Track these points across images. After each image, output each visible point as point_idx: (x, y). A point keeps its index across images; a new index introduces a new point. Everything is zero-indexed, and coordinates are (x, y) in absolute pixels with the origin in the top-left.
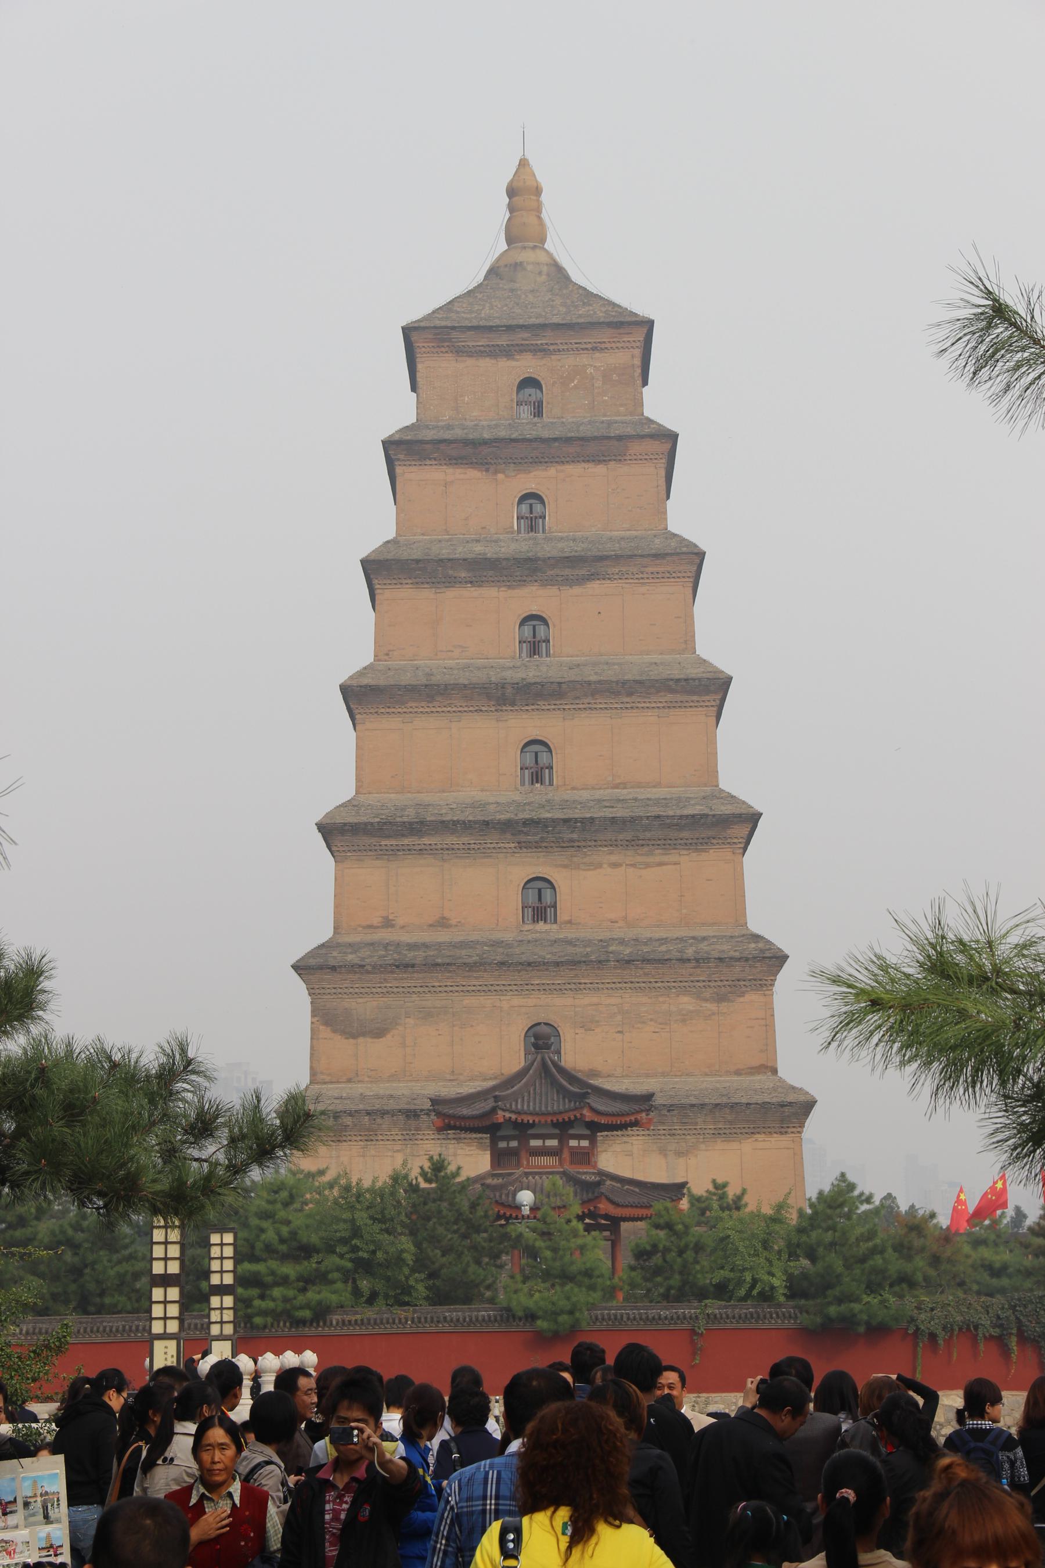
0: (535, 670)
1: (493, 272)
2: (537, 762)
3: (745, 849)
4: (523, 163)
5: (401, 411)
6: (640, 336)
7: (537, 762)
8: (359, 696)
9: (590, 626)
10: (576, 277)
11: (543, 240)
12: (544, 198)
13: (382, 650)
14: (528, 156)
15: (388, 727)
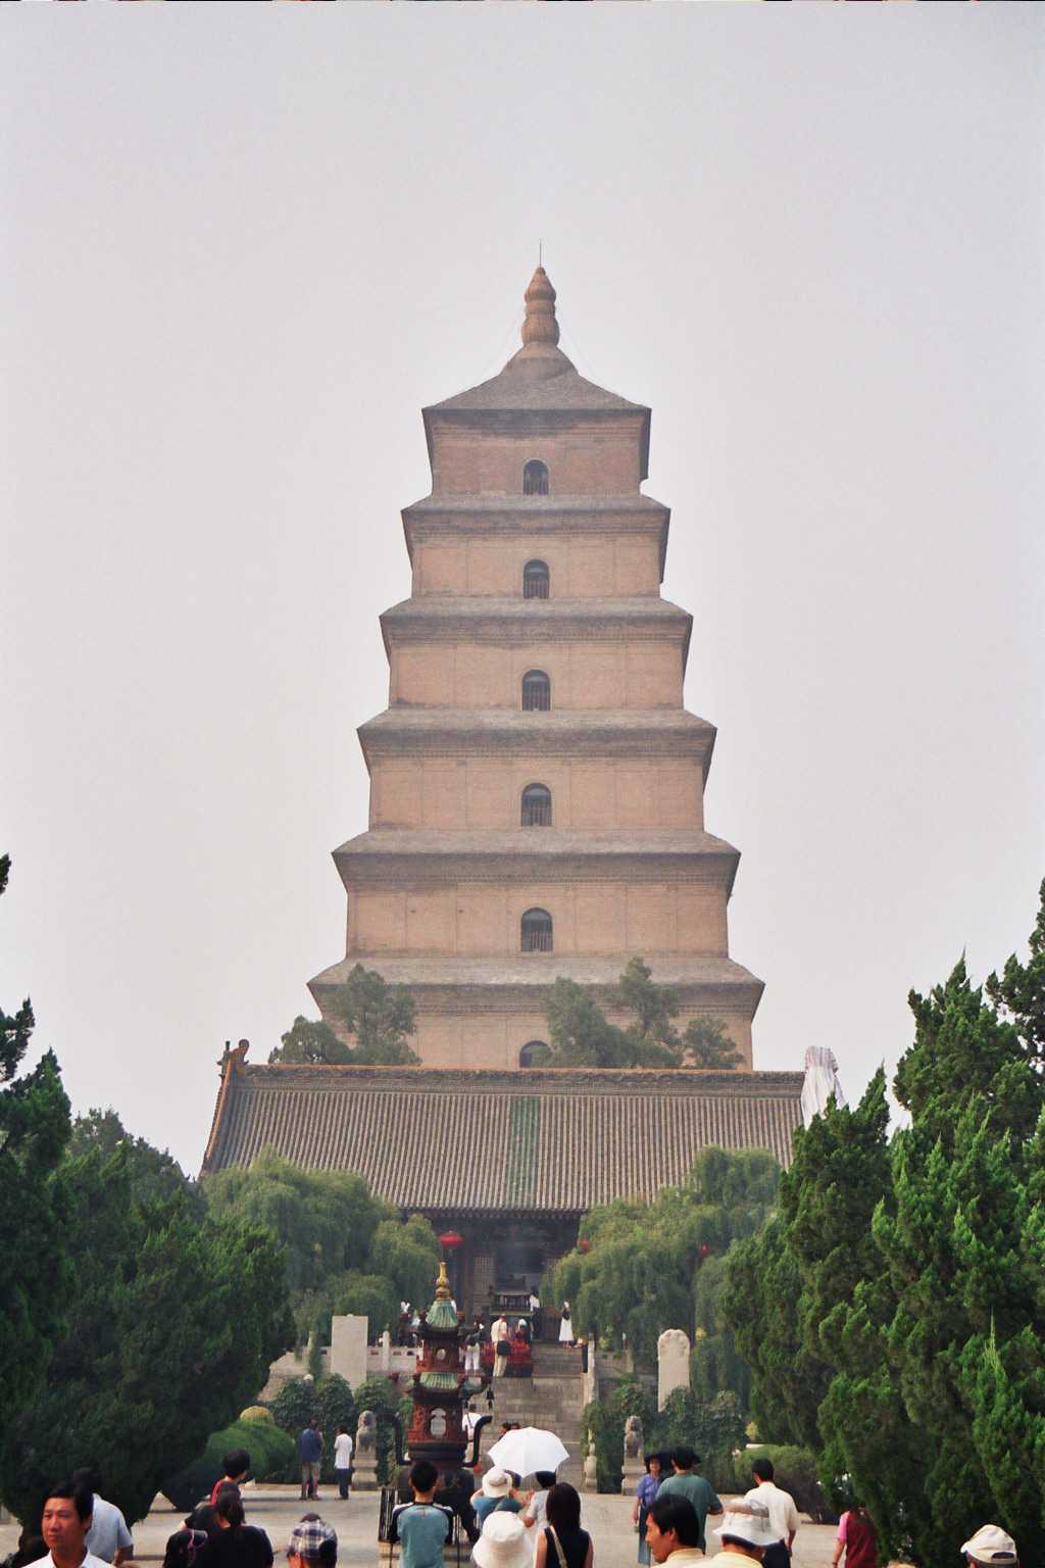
0: (537, 720)
1: (510, 366)
2: (536, 806)
3: (729, 895)
4: (541, 271)
5: (418, 485)
6: (637, 423)
7: (536, 806)
8: (369, 737)
9: (592, 685)
10: (583, 372)
11: (557, 343)
12: (557, 303)
13: (397, 702)
14: (543, 266)
15: (400, 771)
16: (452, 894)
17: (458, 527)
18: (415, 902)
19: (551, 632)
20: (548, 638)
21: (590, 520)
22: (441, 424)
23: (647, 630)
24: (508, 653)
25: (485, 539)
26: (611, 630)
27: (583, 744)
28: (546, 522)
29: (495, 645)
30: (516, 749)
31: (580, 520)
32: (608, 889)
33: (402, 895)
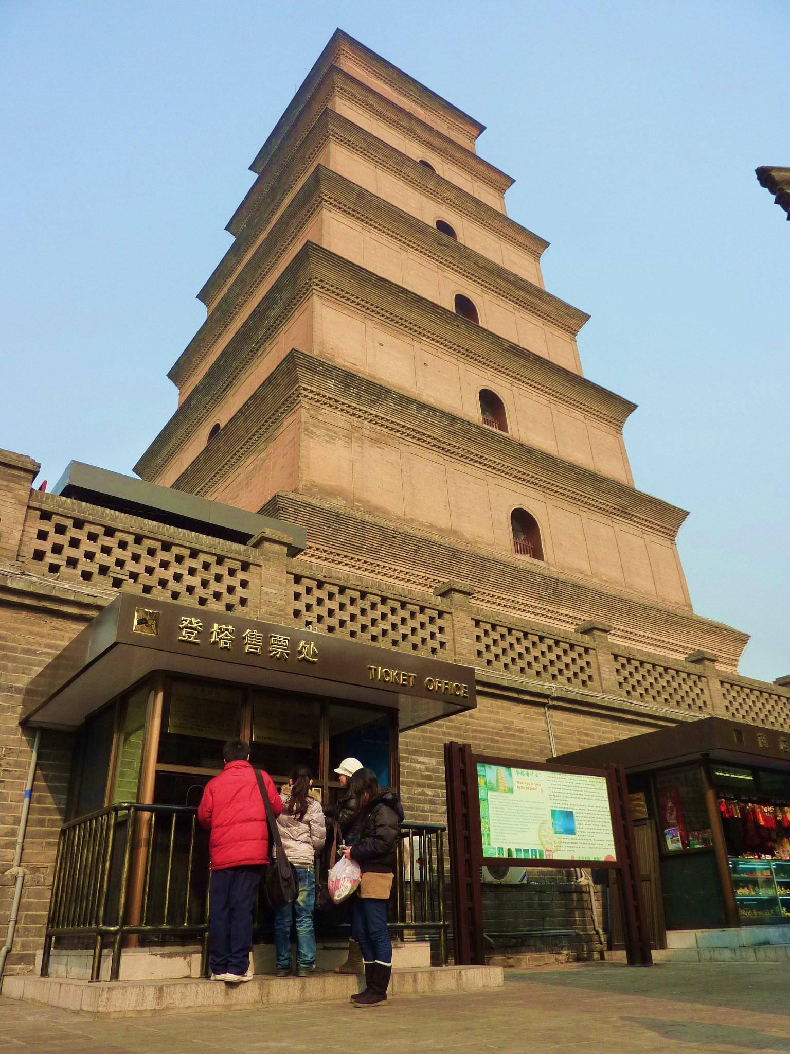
16: (416, 345)
17: (371, 106)
18: (382, 336)
19: (456, 202)
20: (452, 205)
21: (464, 158)
22: (346, 48)
23: (520, 238)
24: (425, 199)
25: (390, 128)
26: (497, 224)
27: (500, 282)
28: (437, 142)
29: (415, 189)
30: (450, 259)
31: (458, 155)
32: (543, 399)
33: (370, 324)
